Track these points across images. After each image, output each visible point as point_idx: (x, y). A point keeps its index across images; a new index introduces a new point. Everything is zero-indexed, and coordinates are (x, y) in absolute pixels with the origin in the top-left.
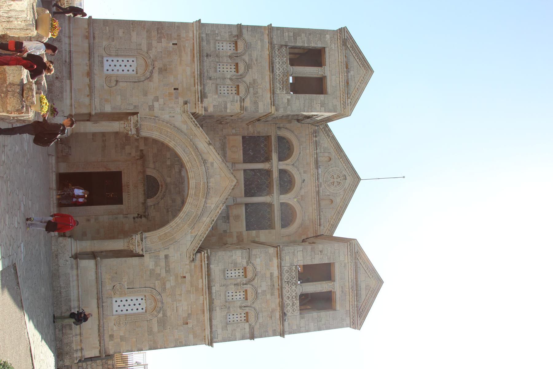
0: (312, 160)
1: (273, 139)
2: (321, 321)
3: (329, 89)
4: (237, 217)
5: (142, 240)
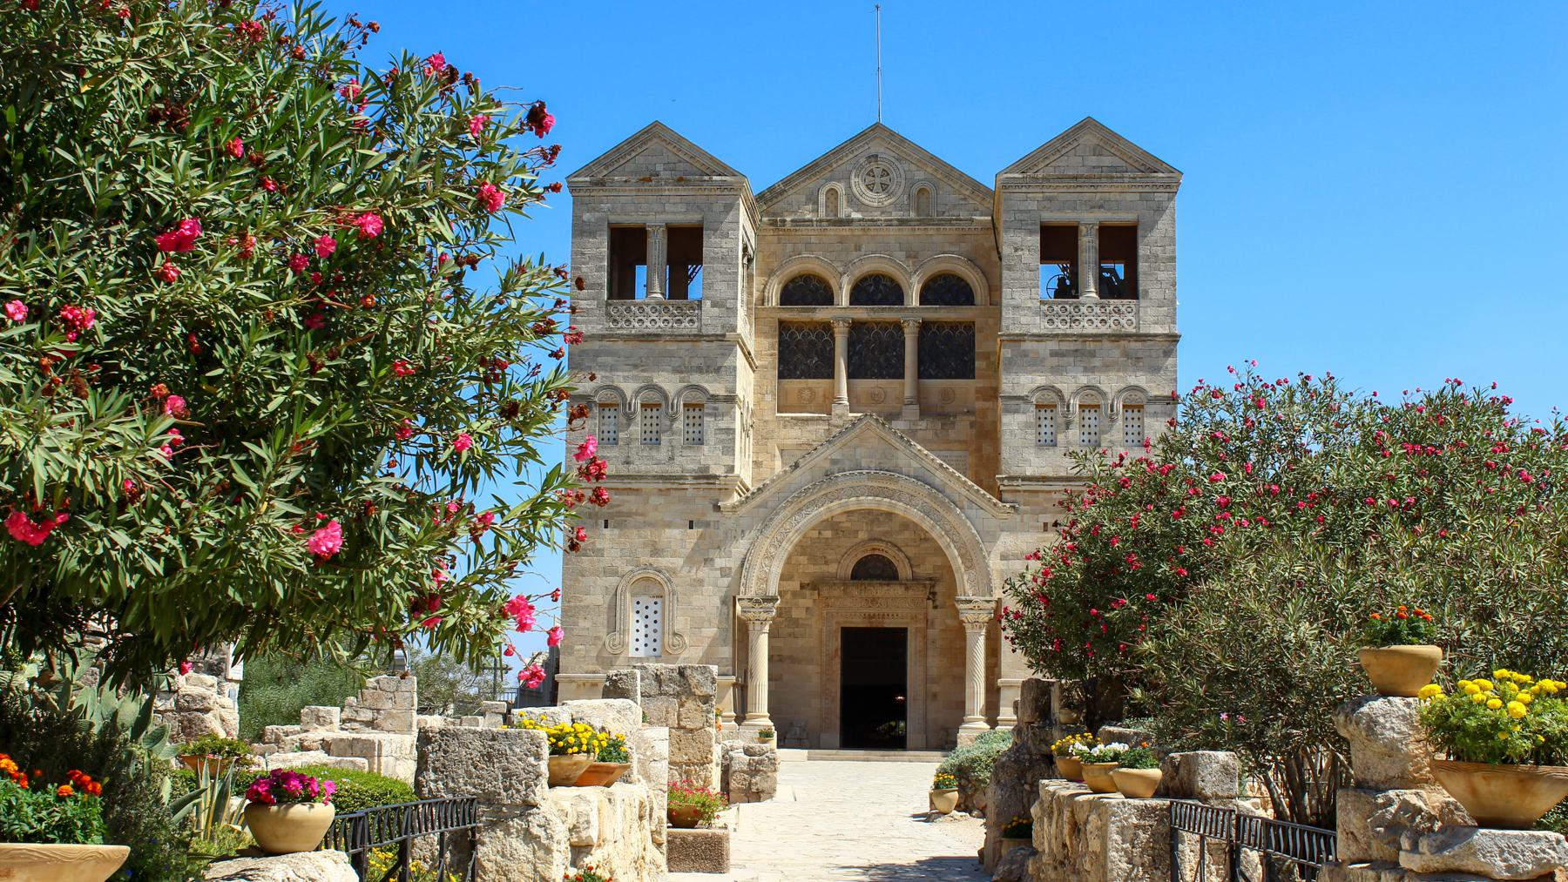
0: (833, 231)
1: (786, 316)
2: (1156, 256)
3: (691, 218)
4: (947, 395)
5: (970, 601)
